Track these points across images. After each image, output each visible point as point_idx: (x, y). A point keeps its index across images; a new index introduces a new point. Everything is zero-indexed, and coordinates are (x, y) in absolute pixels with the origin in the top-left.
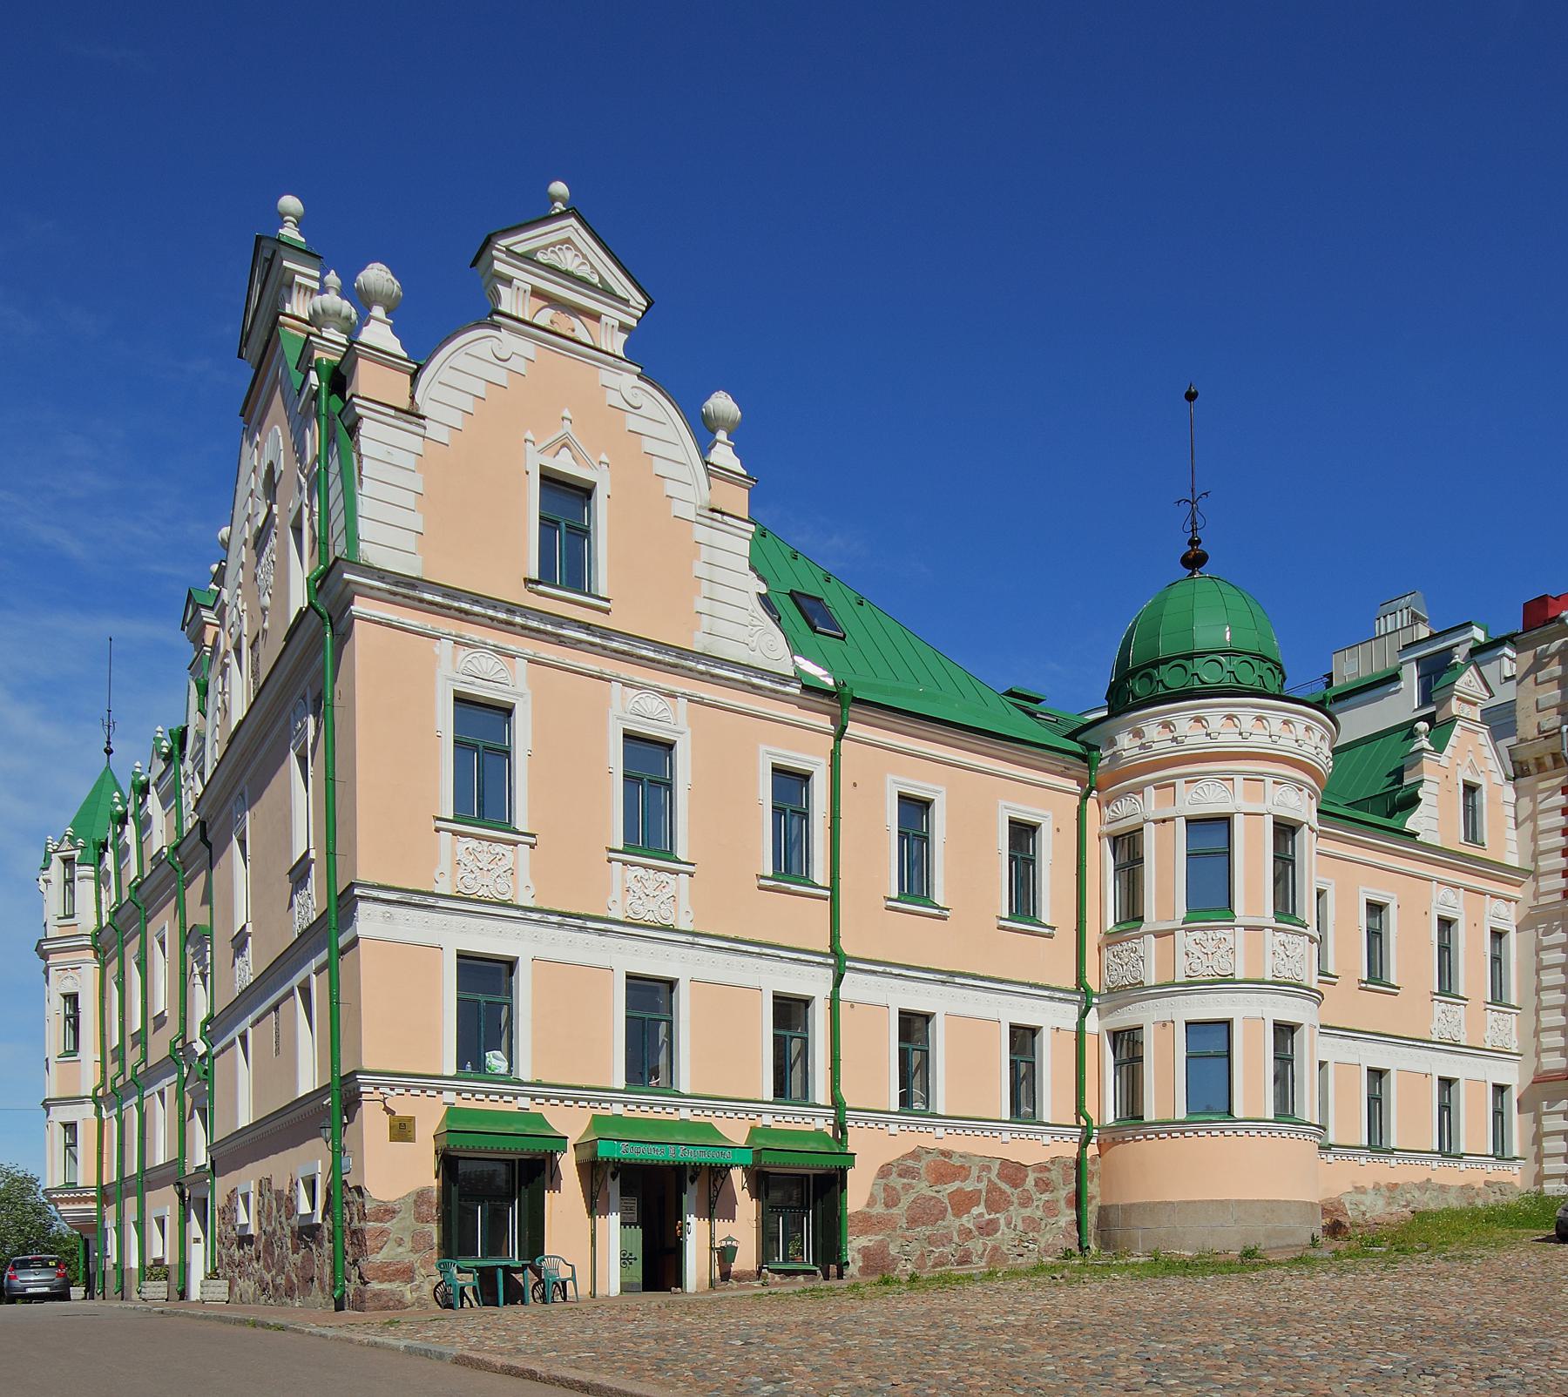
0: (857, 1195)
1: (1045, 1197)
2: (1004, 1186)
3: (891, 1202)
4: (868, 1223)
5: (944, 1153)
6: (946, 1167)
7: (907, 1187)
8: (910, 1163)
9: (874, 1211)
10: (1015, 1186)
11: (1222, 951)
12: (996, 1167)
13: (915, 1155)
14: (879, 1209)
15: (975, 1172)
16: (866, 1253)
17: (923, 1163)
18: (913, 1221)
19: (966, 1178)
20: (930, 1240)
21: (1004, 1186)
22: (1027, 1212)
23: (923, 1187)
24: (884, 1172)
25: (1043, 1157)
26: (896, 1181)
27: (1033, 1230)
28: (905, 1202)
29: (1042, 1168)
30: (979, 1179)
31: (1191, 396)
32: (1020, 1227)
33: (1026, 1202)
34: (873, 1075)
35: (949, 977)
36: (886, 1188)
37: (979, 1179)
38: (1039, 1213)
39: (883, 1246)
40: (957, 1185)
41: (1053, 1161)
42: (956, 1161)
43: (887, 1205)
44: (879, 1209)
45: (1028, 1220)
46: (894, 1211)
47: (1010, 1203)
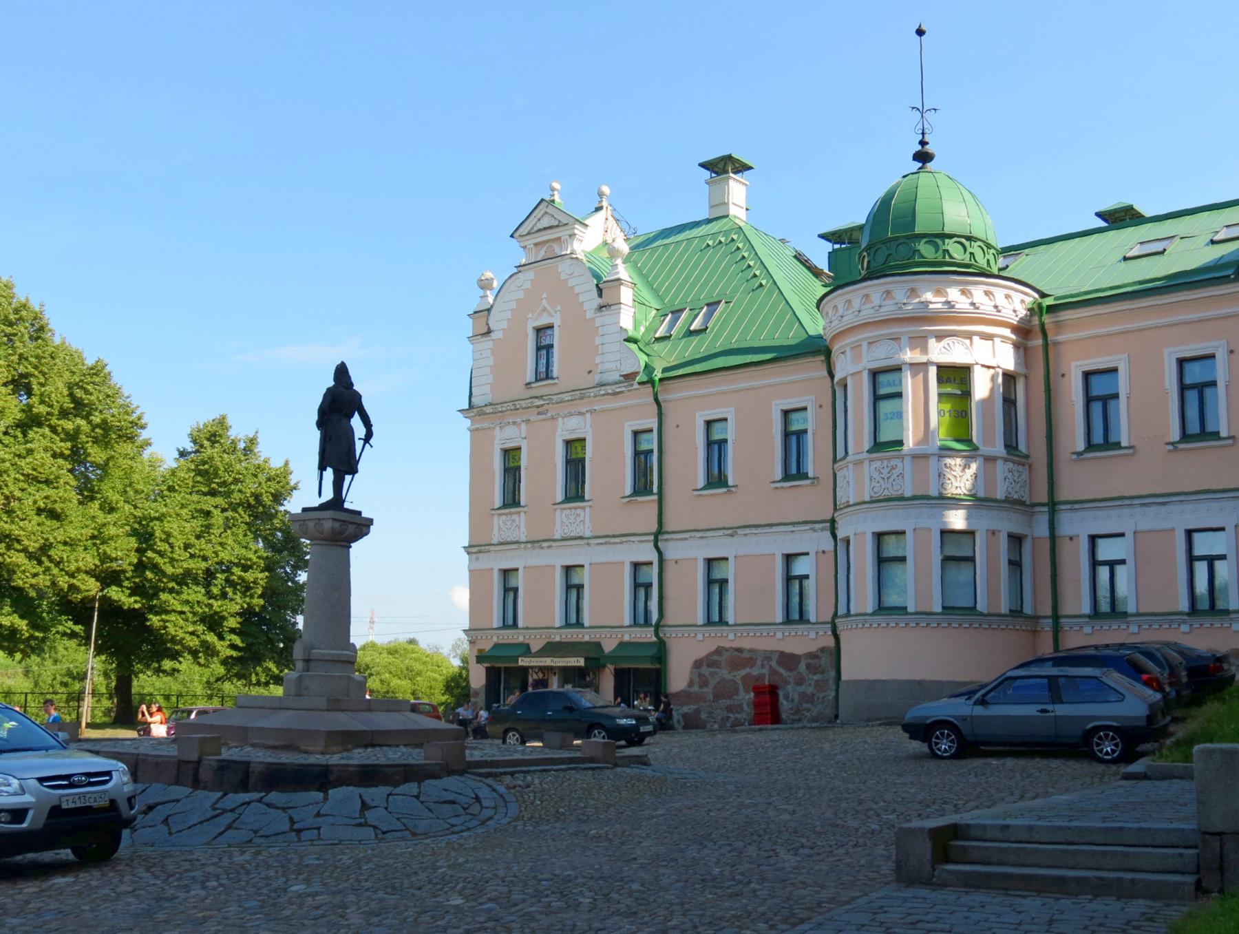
0: (678, 678)
1: (816, 677)
2: (781, 670)
3: (704, 683)
4: (685, 696)
5: (739, 650)
6: (739, 658)
7: (713, 675)
8: (715, 657)
9: (692, 690)
10: (791, 670)
11: (895, 476)
12: (775, 657)
13: (719, 651)
14: (696, 688)
15: (759, 662)
16: (685, 716)
17: (724, 657)
18: (717, 697)
19: (752, 666)
20: (729, 709)
21: (781, 670)
22: (802, 689)
23: (725, 673)
24: (698, 664)
25: (813, 648)
26: (705, 670)
27: (807, 702)
28: (713, 682)
29: (810, 655)
30: (763, 666)
31: (920, 32)
32: (796, 697)
33: (800, 681)
34: (686, 601)
35: (732, 531)
36: (700, 675)
37: (763, 666)
38: (810, 690)
39: (698, 712)
40: (747, 670)
41: (823, 650)
42: (746, 655)
43: (700, 687)
44: (696, 688)
45: (803, 695)
46: (706, 690)
47: (786, 683)
